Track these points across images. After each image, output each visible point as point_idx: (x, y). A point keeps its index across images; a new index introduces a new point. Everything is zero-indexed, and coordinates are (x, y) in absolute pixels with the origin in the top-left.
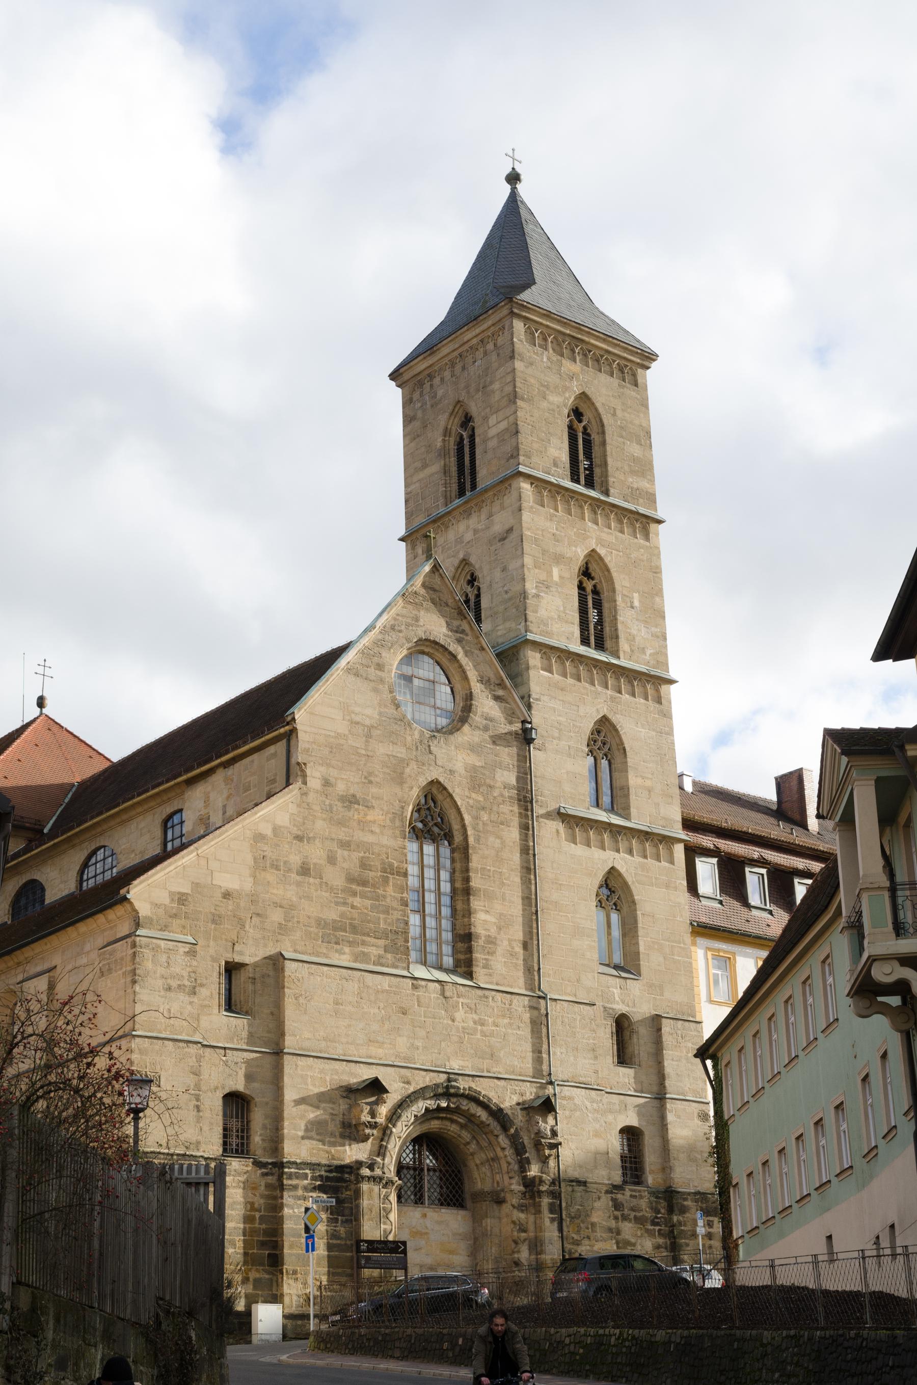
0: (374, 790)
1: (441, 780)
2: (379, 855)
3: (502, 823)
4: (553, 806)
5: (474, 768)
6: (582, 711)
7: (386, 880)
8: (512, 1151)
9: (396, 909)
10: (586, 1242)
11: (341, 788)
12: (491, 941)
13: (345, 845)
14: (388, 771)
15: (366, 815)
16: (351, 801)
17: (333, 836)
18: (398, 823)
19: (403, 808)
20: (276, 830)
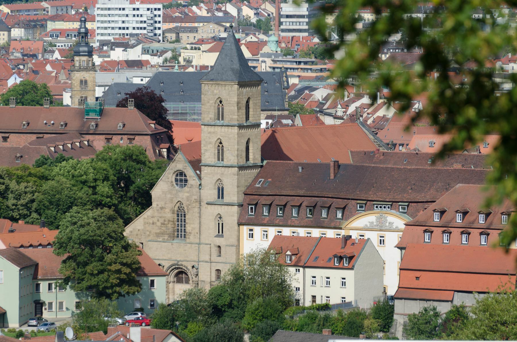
0: (167, 205)
4: (206, 202)
5: (188, 197)
11: (160, 206)
12: (190, 233)
13: (161, 217)
16: (162, 208)
20: (148, 217)
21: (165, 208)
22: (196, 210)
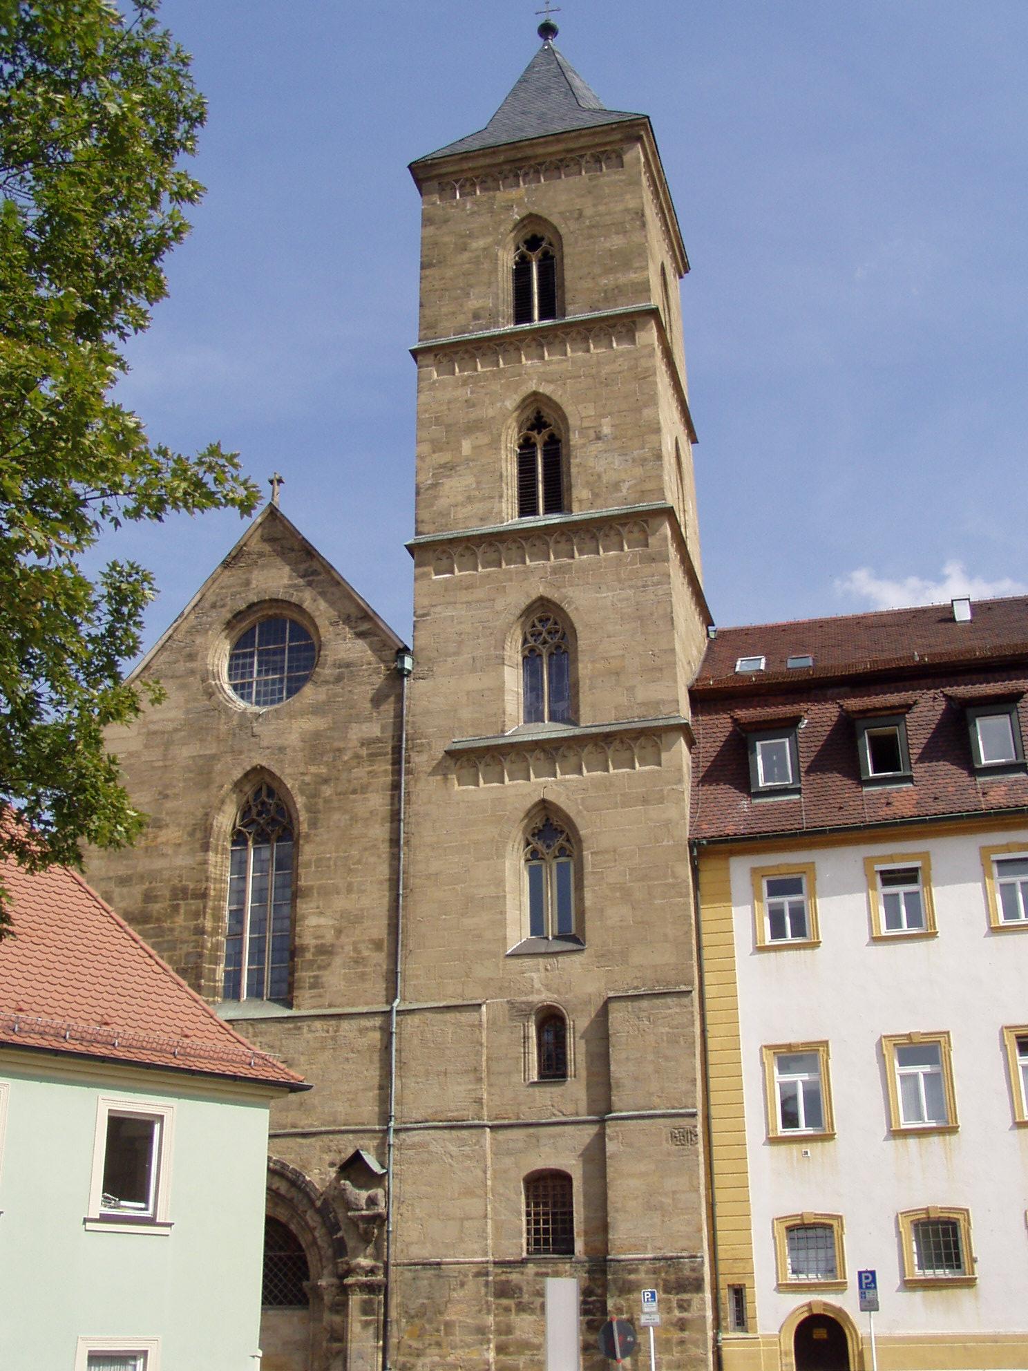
0: (169, 805)
1: (264, 764)
2: (169, 880)
3: (354, 792)
5: (317, 735)
6: (500, 604)
7: (175, 909)
8: (323, 1230)
9: (187, 942)
10: (435, 1351)
13: (124, 881)
14: (191, 775)
15: (156, 837)
17: (111, 874)
18: (199, 835)
19: (207, 814)
21: (158, 825)
22: (378, 801)
